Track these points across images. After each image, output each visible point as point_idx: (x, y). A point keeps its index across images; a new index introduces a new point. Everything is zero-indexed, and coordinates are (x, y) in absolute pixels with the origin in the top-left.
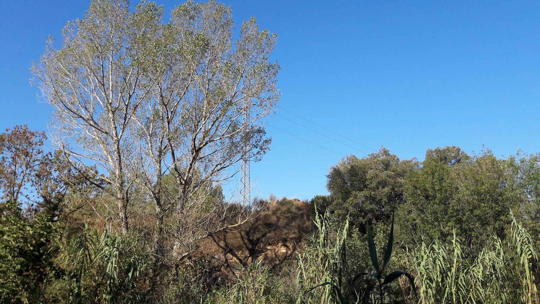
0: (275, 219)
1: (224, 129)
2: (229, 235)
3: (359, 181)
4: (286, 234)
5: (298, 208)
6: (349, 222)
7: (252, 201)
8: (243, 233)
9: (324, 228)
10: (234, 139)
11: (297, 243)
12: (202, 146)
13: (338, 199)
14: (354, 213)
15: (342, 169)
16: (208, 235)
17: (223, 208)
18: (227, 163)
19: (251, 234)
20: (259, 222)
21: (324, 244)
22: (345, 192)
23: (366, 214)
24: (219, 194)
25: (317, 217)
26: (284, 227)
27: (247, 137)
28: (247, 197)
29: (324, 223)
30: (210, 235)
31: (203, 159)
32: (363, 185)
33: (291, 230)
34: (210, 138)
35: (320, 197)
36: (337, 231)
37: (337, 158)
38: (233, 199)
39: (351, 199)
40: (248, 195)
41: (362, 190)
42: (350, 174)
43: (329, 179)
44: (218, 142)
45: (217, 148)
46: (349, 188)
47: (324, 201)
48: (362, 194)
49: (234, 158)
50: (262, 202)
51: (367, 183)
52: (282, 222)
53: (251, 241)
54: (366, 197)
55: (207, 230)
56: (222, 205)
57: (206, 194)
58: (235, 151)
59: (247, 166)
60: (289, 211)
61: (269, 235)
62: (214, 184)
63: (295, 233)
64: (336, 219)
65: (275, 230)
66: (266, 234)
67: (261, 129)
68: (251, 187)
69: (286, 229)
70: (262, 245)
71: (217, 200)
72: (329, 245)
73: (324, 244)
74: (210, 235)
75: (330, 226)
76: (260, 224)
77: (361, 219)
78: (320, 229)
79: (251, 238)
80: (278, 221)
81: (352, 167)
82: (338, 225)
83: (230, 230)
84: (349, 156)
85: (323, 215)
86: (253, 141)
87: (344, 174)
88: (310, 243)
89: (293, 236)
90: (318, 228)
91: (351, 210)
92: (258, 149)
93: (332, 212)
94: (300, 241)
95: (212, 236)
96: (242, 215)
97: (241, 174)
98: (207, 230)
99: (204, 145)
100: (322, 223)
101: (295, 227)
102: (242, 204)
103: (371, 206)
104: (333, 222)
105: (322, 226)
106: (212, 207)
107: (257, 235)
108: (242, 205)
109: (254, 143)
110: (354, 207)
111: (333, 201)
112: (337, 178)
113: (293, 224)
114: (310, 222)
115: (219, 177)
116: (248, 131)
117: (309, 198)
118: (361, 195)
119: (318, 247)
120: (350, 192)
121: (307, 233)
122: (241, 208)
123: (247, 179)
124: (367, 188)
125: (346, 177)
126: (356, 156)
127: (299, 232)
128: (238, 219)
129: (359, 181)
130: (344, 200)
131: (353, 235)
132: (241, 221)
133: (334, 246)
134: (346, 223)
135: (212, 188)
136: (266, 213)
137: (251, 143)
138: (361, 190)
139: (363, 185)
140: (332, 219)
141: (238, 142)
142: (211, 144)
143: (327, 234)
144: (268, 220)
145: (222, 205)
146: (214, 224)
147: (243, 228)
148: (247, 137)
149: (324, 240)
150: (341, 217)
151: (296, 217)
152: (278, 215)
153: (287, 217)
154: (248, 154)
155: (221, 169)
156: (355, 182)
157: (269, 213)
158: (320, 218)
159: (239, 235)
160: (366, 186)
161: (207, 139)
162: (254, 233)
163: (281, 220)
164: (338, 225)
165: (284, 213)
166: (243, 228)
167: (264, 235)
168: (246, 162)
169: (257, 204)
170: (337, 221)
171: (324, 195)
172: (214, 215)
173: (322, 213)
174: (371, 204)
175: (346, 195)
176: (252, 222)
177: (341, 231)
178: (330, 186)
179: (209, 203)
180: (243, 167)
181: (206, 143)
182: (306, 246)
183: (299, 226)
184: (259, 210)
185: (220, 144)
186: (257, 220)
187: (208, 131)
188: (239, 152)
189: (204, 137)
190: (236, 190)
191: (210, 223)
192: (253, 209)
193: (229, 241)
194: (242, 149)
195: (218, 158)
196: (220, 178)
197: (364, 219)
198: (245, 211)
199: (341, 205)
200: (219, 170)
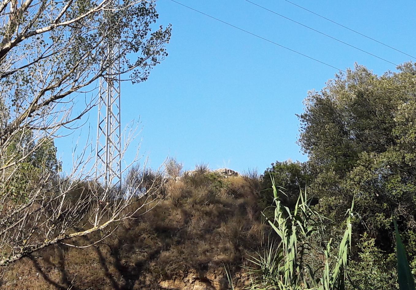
0: (179, 217)
1: (59, 6)
2: (72, 255)
3: (377, 127)
4: (205, 252)
5: (234, 192)
6: (354, 224)
7: (125, 175)
8: (104, 251)
9: (293, 237)
10: (84, 30)
11: (232, 274)
12: (8, 46)
13: (328, 170)
14: (364, 204)
15: (335, 99)
16: (23, 256)
17: (57, 192)
18: (67, 86)
19: (122, 254)
20: (142, 225)
21: (295, 276)
22: (345, 155)
23: (393, 206)
24: (49, 159)
25: (277, 212)
26: (202, 237)
27: (114, 25)
28: (114, 165)
29: (294, 228)
30: (28, 254)
31: (11, 76)
32: (386, 139)
33: (217, 244)
34: (27, 28)
35: (285, 165)
36: (324, 246)
37: (325, 77)
38: (80, 169)
39: (356, 170)
40: (117, 160)
41: (384, 150)
42: (355, 111)
43: (306, 125)
44: (46, 38)
45: (43, 50)
46: (353, 144)
47: (294, 175)
48: (383, 158)
49: (85, 73)
50: (148, 178)
51: (395, 132)
52: (195, 226)
53: (122, 270)
54: (393, 167)
55: (20, 243)
56: (55, 183)
57: (17, 158)
58: (85, 58)
59: (114, 94)
60: (212, 198)
61: (165, 254)
62: (37, 136)
63: (225, 250)
64: (322, 217)
65: (179, 243)
66: (158, 252)
67: (147, 6)
68: (124, 144)
69: (205, 240)
70: (148, 279)
71: (43, 172)
72: (305, 278)
73: (295, 276)
74: (28, 254)
75: (309, 234)
76: (144, 230)
77: (381, 217)
78: (285, 241)
79: (123, 261)
80: (187, 222)
81: (360, 95)
82: (327, 232)
83: (74, 243)
84: (353, 70)
85: (292, 209)
86: (127, 34)
87: (342, 111)
88: (261, 273)
89: (222, 257)
90: (280, 239)
91: (358, 195)
92: (140, 54)
93: (313, 202)
94: (239, 269)
95: (32, 258)
96: (102, 207)
97: (100, 112)
98: (20, 243)
99: (13, 45)
100: (289, 226)
101: (226, 236)
102: (102, 181)
103: (404, 188)
104: (315, 225)
105: (289, 234)
106: (31, 189)
107: (138, 256)
108: (103, 185)
109: (129, 40)
110: (365, 190)
111: (315, 173)
112: (324, 122)
113: (222, 229)
114: (262, 225)
115: (48, 118)
116: (115, 10)
117: (260, 169)
118: (381, 160)
119: (280, 283)
120: (355, 153)
121: (255, 249)
122: (100, 191)
123: (115, 124)
124: (395, 144)
125: (347, 118)
126: (370, 70)
127: (236, 248)
128: (93, 218)
129: (377, 127)
130: (342, 172)
131: (362, 255)
132: (101, 223)
133: (318, 281)
134: (345, 227)
135: (32, 145)
136: (159, 203)
137: (123, 38)
138: (381, 149)
139: (386, 139)
140: (313, 217)
141: (94, 37)
142: (29, 41)
143: (302, 253)
144: (163, 220)
145: (55, 183)
146: (36, 228)
147: (105, 238)
148: (114, 25)
149: (295, 266)
150: (334, 213)
151: (228, 212)
152: (187, 207)
153: (207, 214)
154: (115, 65)
155: (52, 100)
156: (367, 132)
157: (166, 202)
158: (285, 215)
159: (94, 255)
160: (392, 141)
161: (20, 30)
162: (131, 249)
163: (194, 221)
164: (327, 232)
165: (201, 203)
166: (105, 238)
167: (153, 256)
168: (111, 85)
169: (138, 181)
170: (325, 222)
171: (294, 161)
172: (35, 207)
173: (289, 202)
174: (404, 181)
175: (346, 160)
176: (126, 223)
177: (335, 245)
178: (309, 140)
179: (24, 179)
180: (105, 96)
181: (19, 40)
182: (251, 280)
183: (236, 234)
184: (141, 195)
185: (50, 42)
186: (137, 219)
187: (21, 12)
188: (94, 59)
189: (13, 25)
190: (89, 149)
191: (28, 226)
192: (128, 194)
193: (71, 270)
194: (102, 52)
195: (45, 74)
196: (51, 122)
197: (387, 216)
198: (110, 198)
199: (335, 183)
200: (47, 103)
